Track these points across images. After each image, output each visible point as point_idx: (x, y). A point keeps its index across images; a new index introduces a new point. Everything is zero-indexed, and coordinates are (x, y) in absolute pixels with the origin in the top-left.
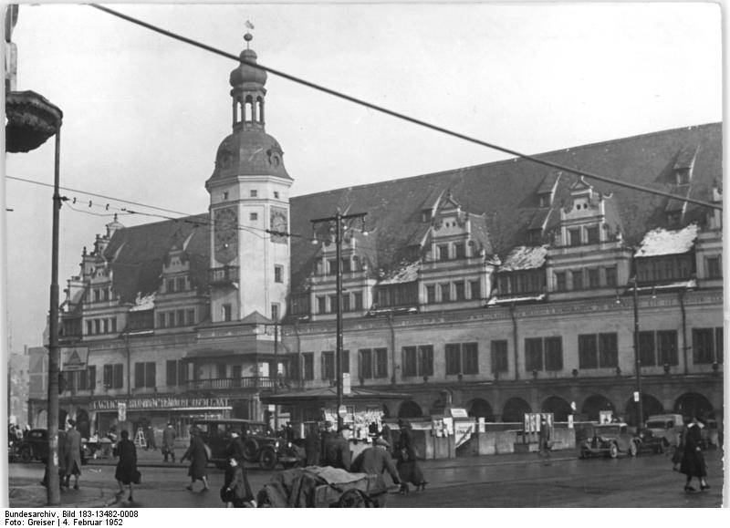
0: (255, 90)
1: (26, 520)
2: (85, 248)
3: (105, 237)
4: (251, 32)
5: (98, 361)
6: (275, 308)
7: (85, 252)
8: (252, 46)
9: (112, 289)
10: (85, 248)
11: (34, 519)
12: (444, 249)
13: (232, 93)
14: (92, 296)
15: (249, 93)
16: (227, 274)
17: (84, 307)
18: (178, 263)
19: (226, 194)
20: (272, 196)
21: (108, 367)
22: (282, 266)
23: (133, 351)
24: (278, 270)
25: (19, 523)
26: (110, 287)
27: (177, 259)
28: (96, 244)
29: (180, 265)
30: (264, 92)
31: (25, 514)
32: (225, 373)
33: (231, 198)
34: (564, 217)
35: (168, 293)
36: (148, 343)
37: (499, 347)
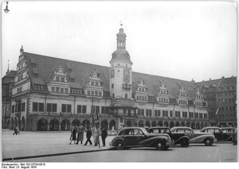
0: (123, 39)
1: (8, 166)
4: (121, 23)
5: (59, 103)
8: (122, 27)
9: (67, 79)
11: (11, 166)
12: (162, 92)
15: (121, 39)
16: (126, 86)
18: (96, 77)
23: (77, 101)
25: (6, 167)
27: (96, 76)
29: (96, 78)
31: (8, 165)
32: (126, 112)
35: (91, 85)
36: (84, 99)
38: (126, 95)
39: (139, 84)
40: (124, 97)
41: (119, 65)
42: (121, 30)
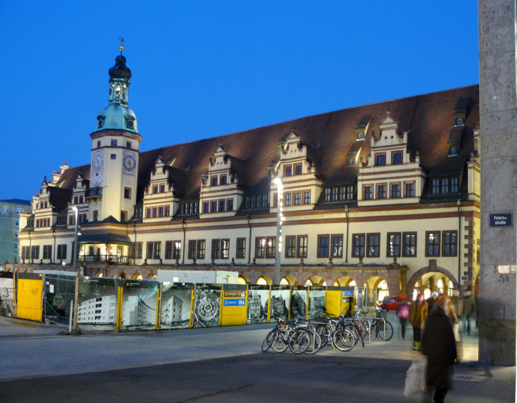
2: (46, 177)
6: (123, 214)
19: (99, 143)
20: (125, 146)
21: (45, 247)
22: (131, 189)
33: (102, 145)
34: (282, 156)
37: (240, 242)
39: (154, 174)
40: (118, 218)
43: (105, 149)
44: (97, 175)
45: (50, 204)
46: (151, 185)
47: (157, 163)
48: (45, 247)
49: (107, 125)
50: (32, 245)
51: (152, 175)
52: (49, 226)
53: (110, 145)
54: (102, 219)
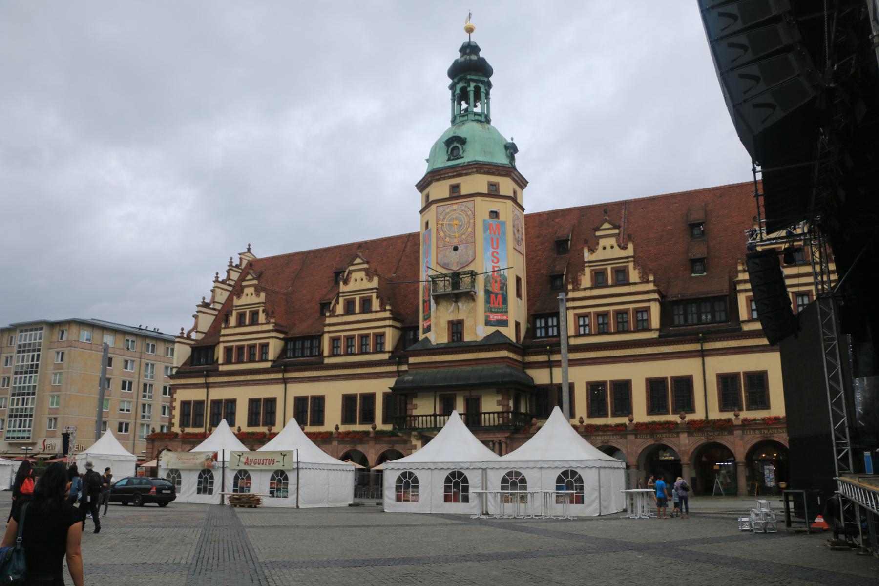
2: (217, 274)
3: (237, 266)
7: (217, 277)
8: (475, 38)
9: (263, 311)
10: (217, 274)
13: (452, 87)
14: (233, 321)
17: (223, 332)
19: (455, 188)
21: (254, 403)
24: (518, 280)
26: (261, 309)
28: (228, 272)
30: (489, 85)
33: (463, 192)
38: (456, 328)
39: (592, 251)
41: (428, 197)
42: (470, 49)
43: (478, 199)
44: (456, 249)
45: (267, 315)
46: (587, 271)
47: (598, 229)
48: (254, 403)
49: (470, 155)
50: (211, 397)
51: (586, 251)
52: (263, 360)
53: (485, 191)
54: (479, 339)
